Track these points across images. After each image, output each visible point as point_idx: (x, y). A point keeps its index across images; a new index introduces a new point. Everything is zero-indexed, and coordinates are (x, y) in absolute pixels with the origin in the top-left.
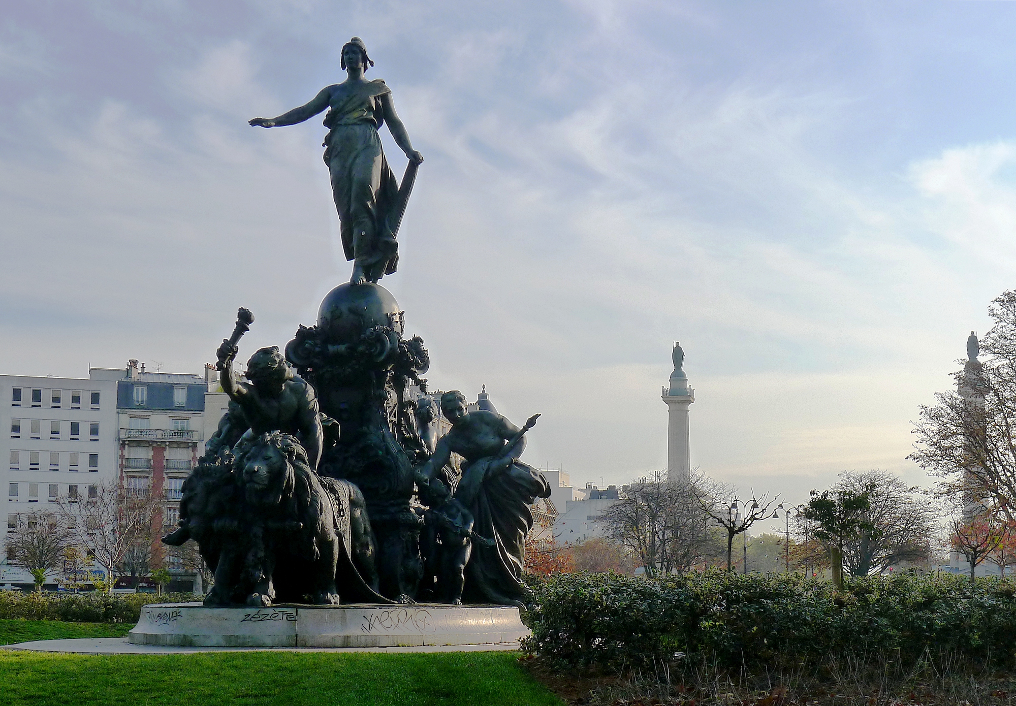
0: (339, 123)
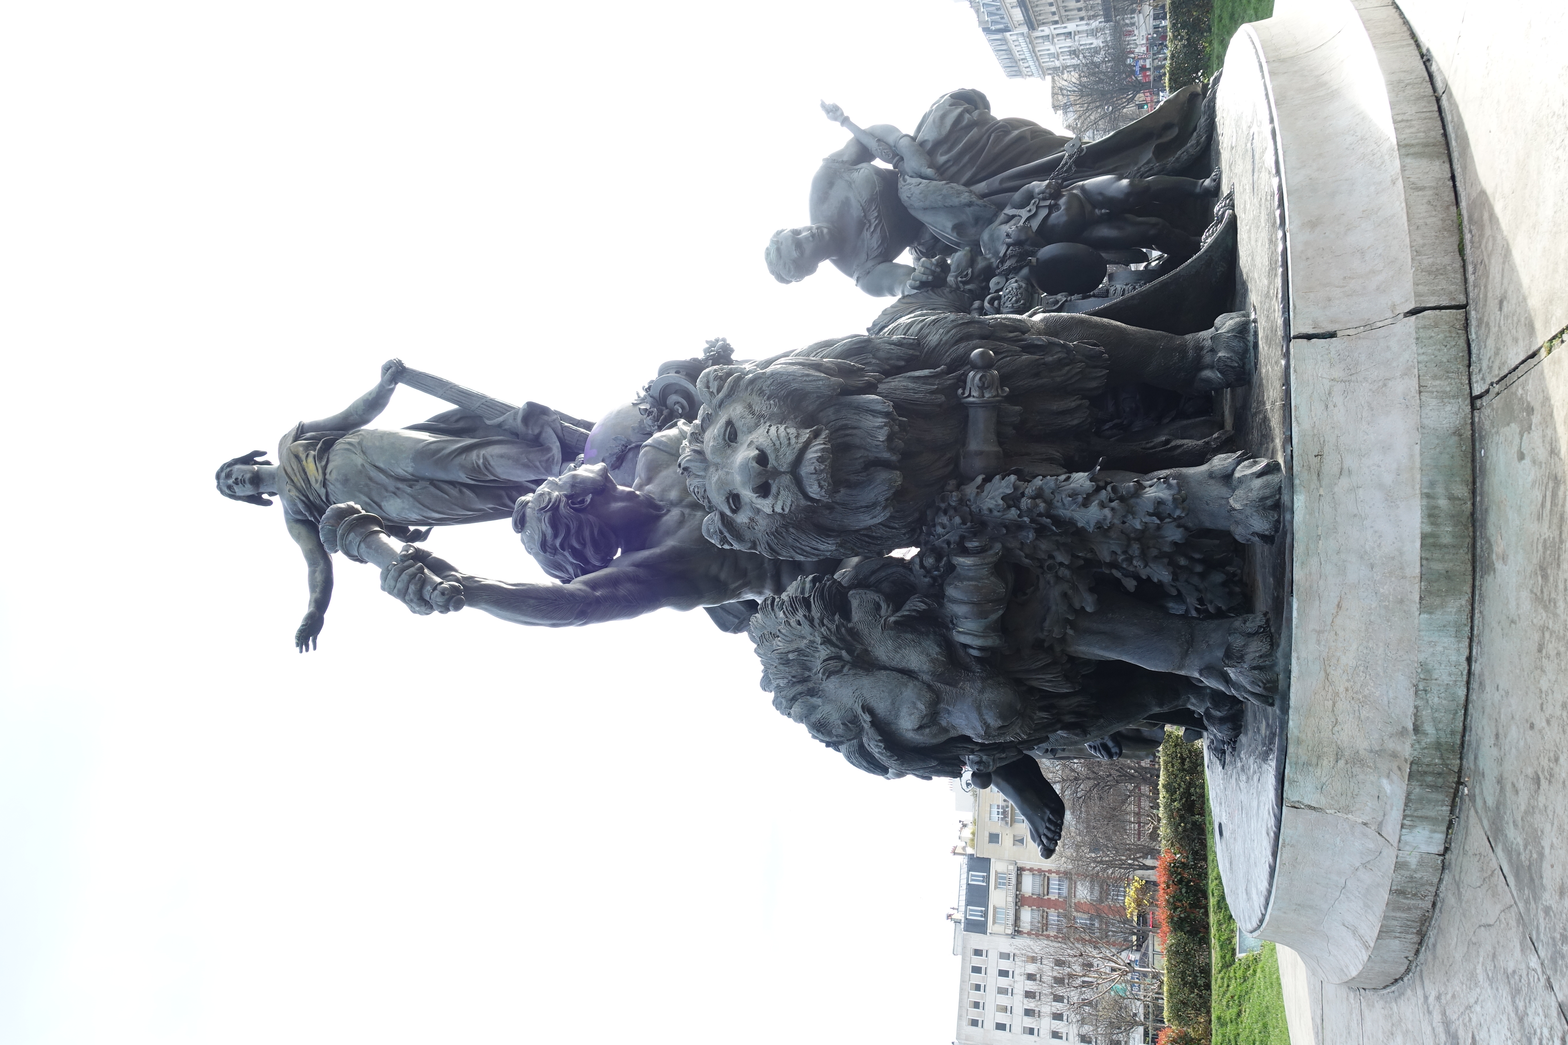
0: (324, 499)
